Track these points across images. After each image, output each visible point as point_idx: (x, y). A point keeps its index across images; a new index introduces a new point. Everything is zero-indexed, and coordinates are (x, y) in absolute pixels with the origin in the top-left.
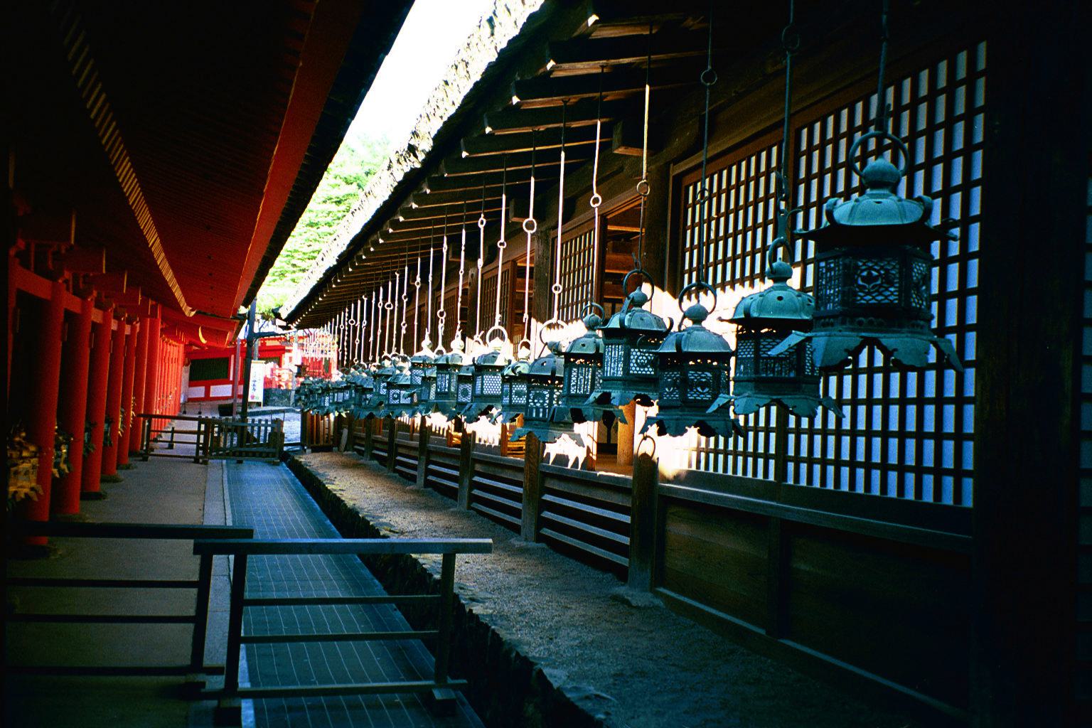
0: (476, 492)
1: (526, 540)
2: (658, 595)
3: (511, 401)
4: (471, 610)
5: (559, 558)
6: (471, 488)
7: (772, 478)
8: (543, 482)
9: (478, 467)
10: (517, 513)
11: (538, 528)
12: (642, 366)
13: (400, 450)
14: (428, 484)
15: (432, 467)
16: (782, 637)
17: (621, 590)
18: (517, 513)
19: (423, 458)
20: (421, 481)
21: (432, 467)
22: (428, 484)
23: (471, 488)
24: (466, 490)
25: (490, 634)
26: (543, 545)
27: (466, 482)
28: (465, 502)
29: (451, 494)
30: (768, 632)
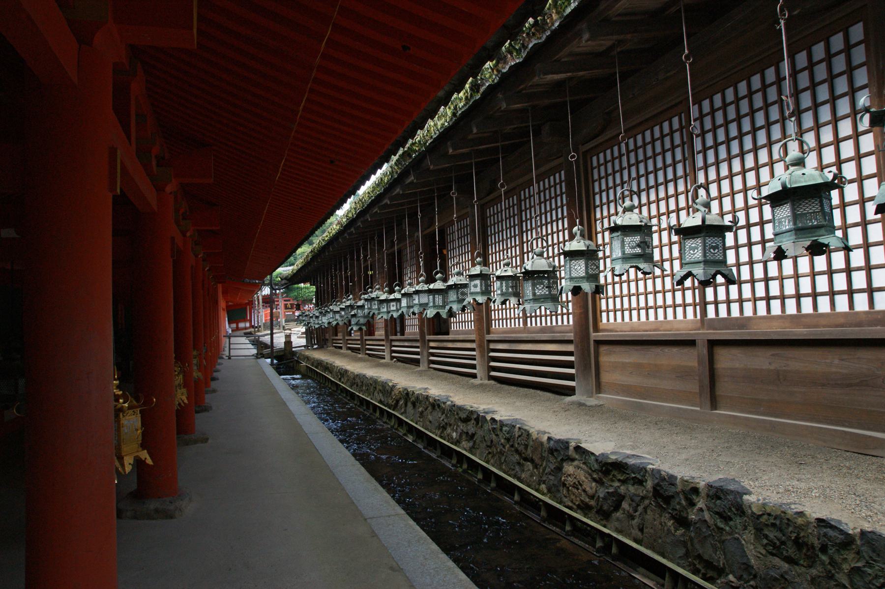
5: (506, 387)
6: (428, 357)
7: (699, 317)
8: (488, 346)
9: (432, 344)
10: (473, 367)
11: (489, 372)
12: (633, 248)
13: (368, 342)
15: (394, 348)
18: (473, 367)
20: (387, 357)
21: (394, 348)
22: (392, 358)
23: (428, 357)
24: (425, 358)
25: (517, 429)
26: (492, 382)
27: (425, 354)
28: (426, 364)
29: (416, 362)
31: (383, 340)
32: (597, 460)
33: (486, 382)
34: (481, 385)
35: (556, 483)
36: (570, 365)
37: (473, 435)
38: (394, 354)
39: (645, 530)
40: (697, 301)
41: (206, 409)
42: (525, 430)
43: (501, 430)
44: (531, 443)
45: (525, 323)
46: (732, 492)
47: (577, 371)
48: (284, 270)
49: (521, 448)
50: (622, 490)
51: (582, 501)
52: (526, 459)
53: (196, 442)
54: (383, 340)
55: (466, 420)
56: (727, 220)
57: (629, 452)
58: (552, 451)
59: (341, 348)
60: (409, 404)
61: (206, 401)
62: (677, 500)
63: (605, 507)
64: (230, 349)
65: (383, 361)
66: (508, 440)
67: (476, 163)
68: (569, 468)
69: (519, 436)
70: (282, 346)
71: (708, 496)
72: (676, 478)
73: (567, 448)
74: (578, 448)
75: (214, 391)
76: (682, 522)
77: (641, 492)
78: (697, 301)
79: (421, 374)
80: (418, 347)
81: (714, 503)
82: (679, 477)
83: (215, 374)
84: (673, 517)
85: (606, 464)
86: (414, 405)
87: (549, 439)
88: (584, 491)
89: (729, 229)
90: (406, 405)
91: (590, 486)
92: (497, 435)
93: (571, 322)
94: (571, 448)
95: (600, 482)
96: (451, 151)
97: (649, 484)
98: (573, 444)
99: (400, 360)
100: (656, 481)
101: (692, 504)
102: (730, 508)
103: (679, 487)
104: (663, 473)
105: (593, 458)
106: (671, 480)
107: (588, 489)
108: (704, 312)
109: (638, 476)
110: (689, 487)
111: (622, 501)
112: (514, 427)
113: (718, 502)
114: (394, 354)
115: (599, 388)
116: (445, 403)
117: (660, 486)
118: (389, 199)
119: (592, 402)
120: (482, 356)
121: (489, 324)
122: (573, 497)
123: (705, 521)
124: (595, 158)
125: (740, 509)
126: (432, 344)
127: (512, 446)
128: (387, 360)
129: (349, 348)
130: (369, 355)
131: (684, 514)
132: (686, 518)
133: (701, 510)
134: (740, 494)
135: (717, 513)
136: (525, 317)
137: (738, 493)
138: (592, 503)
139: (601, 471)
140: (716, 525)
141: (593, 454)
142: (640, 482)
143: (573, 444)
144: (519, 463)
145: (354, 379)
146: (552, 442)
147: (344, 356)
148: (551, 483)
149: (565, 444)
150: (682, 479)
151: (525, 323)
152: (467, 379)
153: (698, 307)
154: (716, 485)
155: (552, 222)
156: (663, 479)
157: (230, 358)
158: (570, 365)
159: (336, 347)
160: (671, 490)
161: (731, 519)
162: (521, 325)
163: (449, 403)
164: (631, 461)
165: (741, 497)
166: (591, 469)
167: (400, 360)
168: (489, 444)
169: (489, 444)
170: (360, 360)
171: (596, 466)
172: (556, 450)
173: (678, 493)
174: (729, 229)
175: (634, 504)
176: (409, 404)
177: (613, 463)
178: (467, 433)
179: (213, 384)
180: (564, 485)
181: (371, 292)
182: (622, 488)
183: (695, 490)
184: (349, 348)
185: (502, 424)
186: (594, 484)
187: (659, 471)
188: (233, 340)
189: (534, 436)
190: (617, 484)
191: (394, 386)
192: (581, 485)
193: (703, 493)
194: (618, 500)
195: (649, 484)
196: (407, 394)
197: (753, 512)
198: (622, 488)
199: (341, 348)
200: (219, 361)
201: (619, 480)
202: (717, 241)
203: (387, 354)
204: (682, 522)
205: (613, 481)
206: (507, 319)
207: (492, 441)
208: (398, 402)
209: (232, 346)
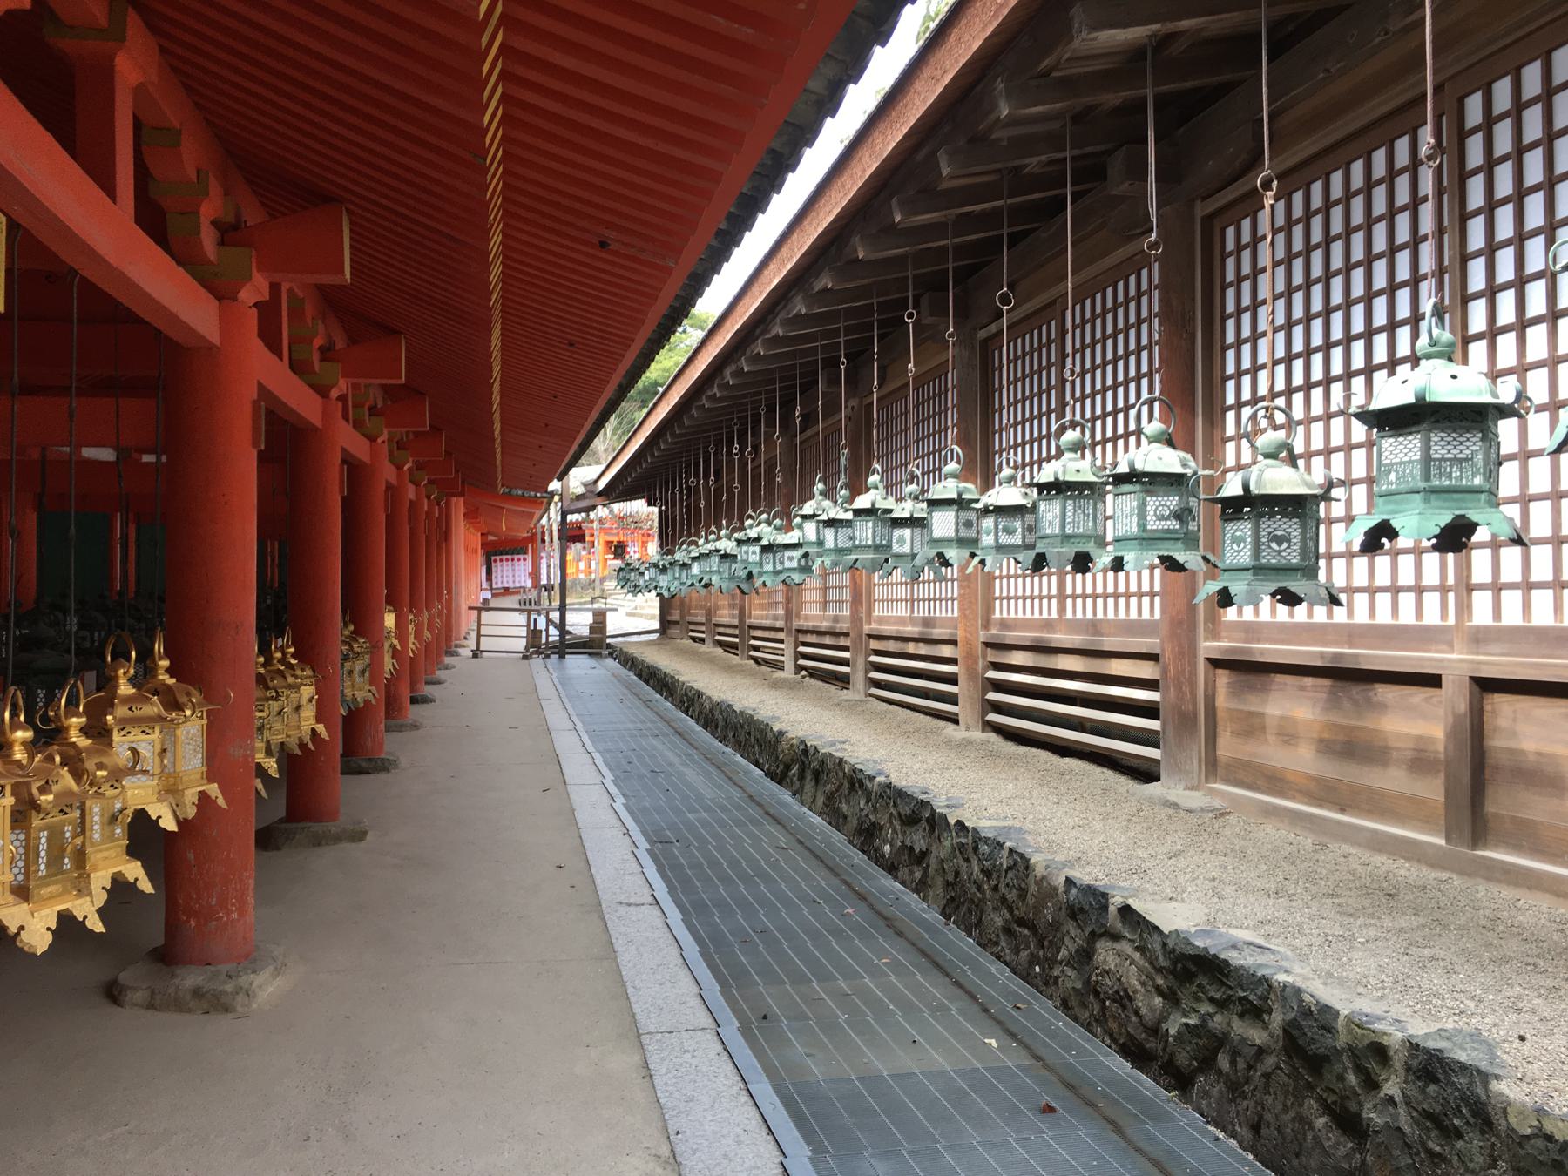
0: (874, 675)
1: (967, 729)
2: (1212, 792)
3: (997, 539)
4: (960, 823)
9: (874, 645)
10: (952, 699)
11: (984, 713)
14: (799, 668)
15: (801, 649)
16: (1486, 846)
17: (1153, 788)
18: (952, 699)
19: (792, 639)
20: (789, 665)
22: (799, 668)
23: (867, 672)
25: (1005, 853)
27: (861, 665)
29: (843, 681)
30: (1448, 840)
31: (781, 630)
32: (1164, 945)
33: (977, 735)
34: (966, 744)
35: (1079, 985)
36: (1150, 710)
37: (924, 854)
38: (801, 662)
39: (1264, 1131)
40: (1451, 580)
41: (383, 766)
42: (1022, 856)
43: (976, 850)
44: (1033, 888)
45: (1062, 609)
46: (1464, 1067)
47: (1163, 726)
48: (580, 477)
49: (1012, 896)
50: (1218, 1022)
51: (1131, 1037)
52: (1021, 922)
53: (338, 839)
54: (781, 630)
55: (911, 821)
56: (1506, 392)
57: (1246, 935)
58: (1074, 912)
59: (702, 640)
60: (809, 776)
61: (386, 748)
62: (1338, 1068)
63: (1182, 1059)
64: (479, 636)
65: (780, 674)
66: (987, 873)
67: (957, 248)
68: (1106, 955)
69: (1009, 868)
70: (585, 632)
71: (1408, 1069)
72: (1337, 1013)
73: (1105, 907)
74: (1126, 911)
75: (415, 727)
76: (1349, 1123)
77: (1258, 1036)
78: (1451, 580)
79: (850, 707)
80: (846, 649)
81: (1423, 1090)
82: (1344, 1012)
83: (428, 690)
84: (1327, 1108)
85: (1184, 957)
86: (817, 776)
87: (1069, 882)
88: (1137, 1013)
89: (1504, 411)
90: (802, 777)
91: (1150, 1004)
92: (967, 860)
93: (1157, 616)
94: (1112, 909)
95: (1171, 997)
96: (897, 219)
97: (1277, 1019)
98: (1116, 901)
99: (813, 673)
100: (1291, 1015)
101: (1372, 1085)
102: (1458, 1107)
103: (1342, 1040)
104: (1307, 998)
105: (1156, 937)
106: (1324, 1016)
107: (1143, 1011)
108: (1464, 608)
109: (1251, 997)
110: (1366, 1042)
111: (1215, 1052)
112: (1001, 845)
113: (1432, 1088)
114: (801, 662)
115: (1212, 767)
116: (872, 778)
117: (1300, 1027)
118: (782, 324)
119: (1195, 799)
120: (972, 674)
121: (989, 609)
122: (1113, 1025)
123: (1399, 1129)
124: (1230, 232)
125: (1484, 1115)
126: (874, 645)
127: (995, 889)
128: (788, 673)
129: (721, 644)
130: (756, 660)
131: (1353, 1107)
132: (1358, 1115)
133: (1391, 1100)
134: (1485, 1077)
135: (1428, 1115)
136: (1062, 597)
137: (1479, 1071)
138: (1151, 1045)
139: (1173, 972)
140: (1423, 1144)
141: (1157, 928)
142: (1256, 1013)
143: (1116, 901)
144: (1008, 931)
145: (711, 710)
146: (1074, 891)
147: (711, 660)
148: (1069, 984)
149: (1099, 898)
150: (1349, 1019)
151: (1062, 609)
152: (942, 724)
153: (1451, 596)
154: (1431, 1044)
155: (1104, 390)
156: (1307, 1013)
157: (475, 656)
158: (1150, 710)
159: (694, 639)
160: (1324, 1043)
161: (1460, 1136)
162: (1054, 615)
163: (880, 779)
164: (1235, 958)
165: (1486, 1084)
166: (1151, 963)
167: (813, 673)
168: (951, 878)
169: (951, 878)
170: (730, 669)
171: (1162, 962)
172: (1082, 910)
173: (1339, 1053)
174: (1504, 411)
175: (1241, 1064)
176: (809, 776)
177: (1198, 956)
178: (912, 849)
179: (414, 712)
180: (1096, 993)
181: (751, 527)
182: (1218, 1018)
183: (1380, 1051)
184: (721, 644)
185: (977, 838)
186: (1158, 1000)
187: (1298, 992)
188: (487, 617)
189: (1040, 871)
190: (1206, 1008)
191: (781, 733)
192: (1130, 999)
193: (1398, 1062)
194: (1210, 1045)
195: (1277, 1019)
196: (806, 751)
197: (1510, 1129)
198: (1218, 1018)
199: (702, 640)
200: (448, 660)
201: (1212, 1000)
202: (1472, 445)
203: (788, 660)
204: (1349, 1123)
205: (1198, 999)
206: (1033, 599)
207: (957, 873)
208: (788, 768)
209: (484, 630)
